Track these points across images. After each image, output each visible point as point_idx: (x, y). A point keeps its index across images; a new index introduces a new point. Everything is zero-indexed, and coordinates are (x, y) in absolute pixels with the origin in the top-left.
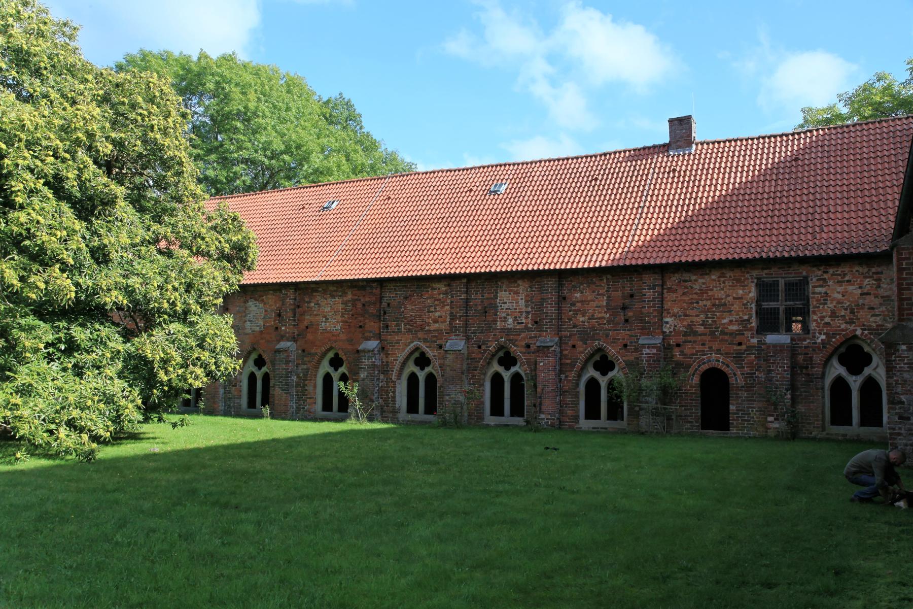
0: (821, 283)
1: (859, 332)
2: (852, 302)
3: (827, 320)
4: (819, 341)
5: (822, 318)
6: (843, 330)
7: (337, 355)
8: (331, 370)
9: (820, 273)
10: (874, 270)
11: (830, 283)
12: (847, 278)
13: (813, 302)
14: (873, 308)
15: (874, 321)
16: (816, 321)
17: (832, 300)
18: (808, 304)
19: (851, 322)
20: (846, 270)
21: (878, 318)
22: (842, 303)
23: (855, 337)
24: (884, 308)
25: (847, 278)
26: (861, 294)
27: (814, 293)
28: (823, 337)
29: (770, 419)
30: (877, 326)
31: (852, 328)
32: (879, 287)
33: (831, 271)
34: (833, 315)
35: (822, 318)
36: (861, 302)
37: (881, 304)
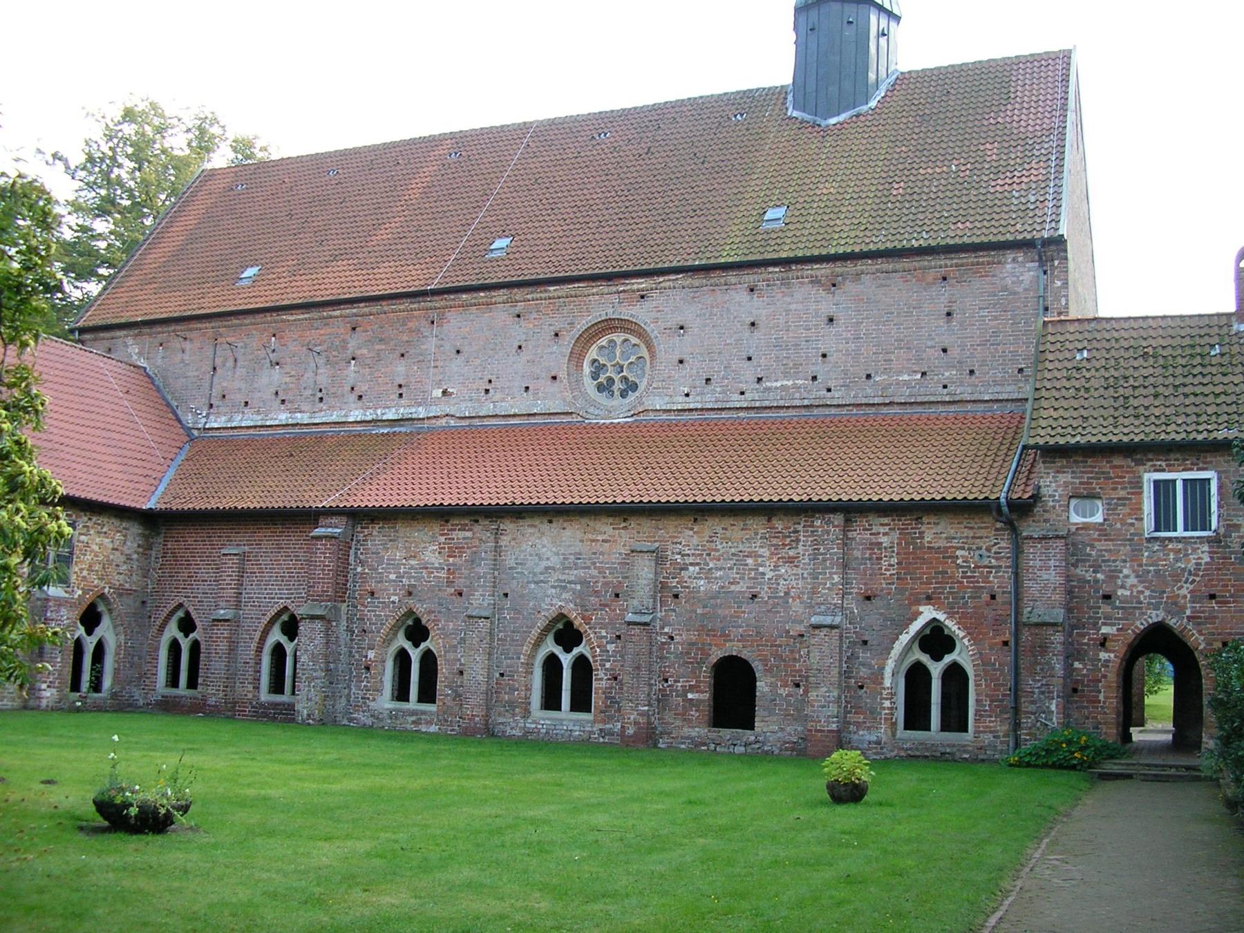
0: (84, 531)
1: (106, 591)
2: (105, 556)
3: (85, 573)
4: (76, 596)
5: (82, 570)
6: (96, 587)
7: (188, 613)
8: (179, 636)
9: (86, 519)
10: (124, 525)
11: (92, 532)
12: (104, 530)
13: (77, 552)
14: (118, 566)
15: (117, 579)
16: (76, 573)
17: (91, 551)
18: (71, 553)
19: (101, 579)
20: (106, 520)
21: (122, 576)
22: (97, 556)
23: (102, 596)
24: (125, 567)
25: (104, 530)
26: (113, 549)
27: (78, 541)
28: (80, 592)
29: (44, 686)
30: (120, 585)
31: (102, 585)
32: (125, 543)
33: (94, 519)
34: (90, 569)
35: (82, 570)
36: (111, 557)
37: (125, 562)
